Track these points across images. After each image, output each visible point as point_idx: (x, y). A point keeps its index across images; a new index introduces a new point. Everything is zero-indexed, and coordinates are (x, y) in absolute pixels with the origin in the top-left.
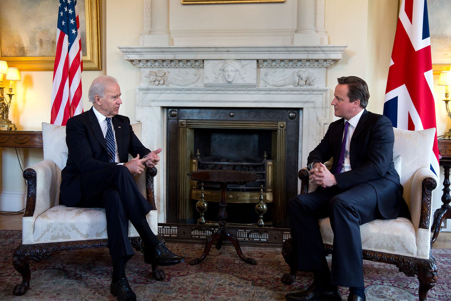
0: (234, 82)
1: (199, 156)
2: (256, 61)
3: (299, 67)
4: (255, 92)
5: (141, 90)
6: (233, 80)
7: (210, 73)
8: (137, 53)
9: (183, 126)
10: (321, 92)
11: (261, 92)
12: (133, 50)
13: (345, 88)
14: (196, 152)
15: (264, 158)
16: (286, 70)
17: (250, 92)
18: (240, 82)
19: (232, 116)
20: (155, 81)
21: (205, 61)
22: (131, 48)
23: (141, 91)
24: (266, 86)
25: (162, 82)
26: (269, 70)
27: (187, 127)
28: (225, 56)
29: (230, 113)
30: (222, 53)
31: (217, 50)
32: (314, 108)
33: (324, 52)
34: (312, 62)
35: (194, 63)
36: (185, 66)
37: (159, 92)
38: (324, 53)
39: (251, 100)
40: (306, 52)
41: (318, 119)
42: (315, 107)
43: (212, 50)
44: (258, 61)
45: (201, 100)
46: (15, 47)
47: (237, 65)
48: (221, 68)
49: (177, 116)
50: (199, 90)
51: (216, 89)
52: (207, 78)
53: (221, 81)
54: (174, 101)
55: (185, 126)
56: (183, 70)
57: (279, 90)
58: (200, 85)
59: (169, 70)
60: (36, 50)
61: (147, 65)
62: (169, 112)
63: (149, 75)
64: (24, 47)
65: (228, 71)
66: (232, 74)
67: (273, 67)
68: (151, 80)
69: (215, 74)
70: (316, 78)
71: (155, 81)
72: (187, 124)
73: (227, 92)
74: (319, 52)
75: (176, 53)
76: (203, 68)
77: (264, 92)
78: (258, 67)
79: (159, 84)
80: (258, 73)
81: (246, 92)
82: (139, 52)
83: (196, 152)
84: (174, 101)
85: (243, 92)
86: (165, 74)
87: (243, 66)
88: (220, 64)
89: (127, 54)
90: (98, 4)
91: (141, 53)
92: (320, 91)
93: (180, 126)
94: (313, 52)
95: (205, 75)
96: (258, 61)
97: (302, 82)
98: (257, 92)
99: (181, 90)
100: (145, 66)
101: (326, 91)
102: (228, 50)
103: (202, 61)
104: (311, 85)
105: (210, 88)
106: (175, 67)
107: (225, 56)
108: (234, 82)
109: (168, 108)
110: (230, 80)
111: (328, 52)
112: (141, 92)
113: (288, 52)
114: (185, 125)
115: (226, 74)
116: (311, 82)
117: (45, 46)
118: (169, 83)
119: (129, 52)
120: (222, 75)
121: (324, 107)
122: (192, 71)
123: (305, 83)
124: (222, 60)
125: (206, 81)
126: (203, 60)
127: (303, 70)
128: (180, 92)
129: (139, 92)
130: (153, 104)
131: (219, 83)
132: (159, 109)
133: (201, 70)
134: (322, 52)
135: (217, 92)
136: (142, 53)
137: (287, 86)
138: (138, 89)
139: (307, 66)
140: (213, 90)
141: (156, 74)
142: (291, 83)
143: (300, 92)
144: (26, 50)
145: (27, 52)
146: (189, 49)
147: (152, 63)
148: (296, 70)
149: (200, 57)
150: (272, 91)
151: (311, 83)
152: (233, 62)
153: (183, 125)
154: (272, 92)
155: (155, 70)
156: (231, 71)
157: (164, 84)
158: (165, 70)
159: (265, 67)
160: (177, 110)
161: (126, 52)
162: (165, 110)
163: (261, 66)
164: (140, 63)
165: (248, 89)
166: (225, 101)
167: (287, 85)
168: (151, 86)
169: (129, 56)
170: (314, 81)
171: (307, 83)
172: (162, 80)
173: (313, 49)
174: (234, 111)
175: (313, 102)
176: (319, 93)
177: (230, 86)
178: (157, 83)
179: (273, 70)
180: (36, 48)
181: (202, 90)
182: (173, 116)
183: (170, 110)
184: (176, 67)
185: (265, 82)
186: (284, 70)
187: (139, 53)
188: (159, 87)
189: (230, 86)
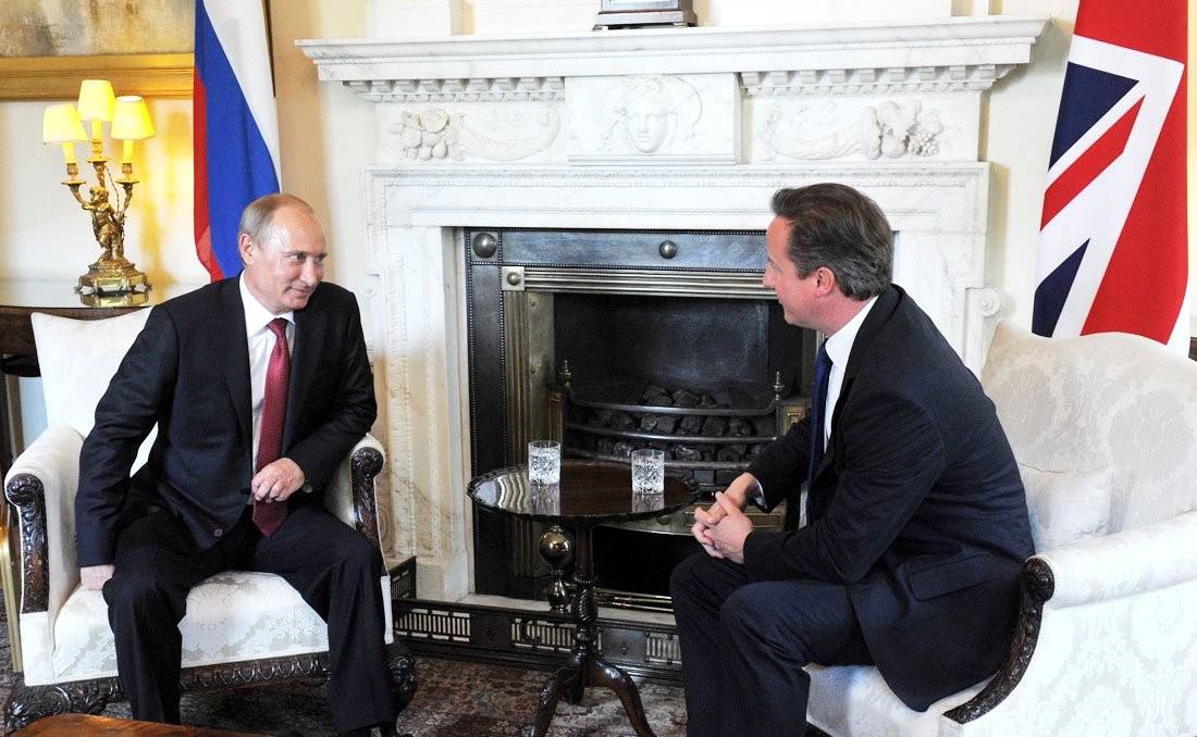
0: (662, 149)
1: (571, 380)
3: (885, 92)
4: (735, 180)
5: (377, 175)
8: (356, 61)
9: (516, 288)
10: (962, 179)
12: (342, 52)
14: (559, 368)
15: (775, 393)
16: (839, 100)
20: (420, 145)
22: (336, 46)
23: (379, 179)
25: (439, 150)
27: (526, 288)
29: (662, 245)
30: (619, 54)
32: (937, 231)
33: (968, 42)
34: (930, 76)
35: (534, 85)
36: (509, 95)
37: (433, 181)
38: (965, 45)
40: (901, 44)
41: (947, 271)
42: (940, 231)
46: (23, 27)
49: (496, 253)
50: (555, 175)
51: (606, 173)
54: (479, 209)
55: (520, 287)
57: (815, 172)
59: (463, 108)
60: (82, 33)
61: (394, 96)
62: (472, 240)
63: (400, 128)
64: (48, 27)
65: (637, 115)
68: (409, 142)
70: (942, 130)
71: (420, 145)
72: (526, 282)
73: (644, 181)
74: (945, 43)
75: (476, 58)
78: (745, 93)
79: (432, 156)
80: (744, 116)
81: (707, 180)
82: (360, 57)
83: (559, 368)
84: (479, 209)
86: (448, 123)
89: (325, 64)
91: (367, 61)
92: (955, 174)
93: (506, 286)
94: (926, 43)
96: (739, 75)
97: (892, 145)
99: (499, 175)
100: (387, 97)
101: (977, 174)
103: (559, 80)
104: (923, 153)
105: (585, 169)
109: (468, 230)
110: (646, 147)
111: (982, 41)
112: (380, 182)
113: (836, 46)
114: (523, 282)
116: (922, 144)
117: (105, 21)
118: (463, 151)
119: (334, 58)
121: (971, 229)
122: (535, 110)
123: (902, 146)
124: (622, 78)
126: (563, 78)
127: (900, 99)
128: (497, 181)
129: (372, 181)
130: (417, 219)
131: (612, 152)
132: (438, 233)
134: (957, 42)
135: (610, 180)
136: (373, 60)
137: (844, 159)
138: (368, 174)
139: (913, 87)
140: (597, 175)
141: (420, 123)
142: (856, 147)
143: (888, 180)
144: (53, 35)
145: (59, 42)
147: (407, 88)
148: (877, 101)
150: (791, 175)
151: (924, 149)
153: (515, 283)
155: (420, 109)
156: (648, 116)
157: (446, 154)
158: (451, 108)
160: (495, 235)
161: (321, 58)
162: (462, 235)
163: (752, 90)
164: (370, 91)
165: (710, 172)
166: (638, 211)
167: (844, 154)
168: (410, 164)
169: (332, 68)
170: (936, 138)
171: (910, 148)
172: (439, 141)
173: (925, 33)
174: (675, 238)
175: (932, 212)
176: (952, 180)
177: (650, 162)
178: (425, 151)
180: (81, 27)
181: (564, 176)
182: (486, 253)
183: (473, 235)
184: (482, 97)
186: (834, 104)
187: (362, 60)
188: (430, 166)
189: (650, 162)
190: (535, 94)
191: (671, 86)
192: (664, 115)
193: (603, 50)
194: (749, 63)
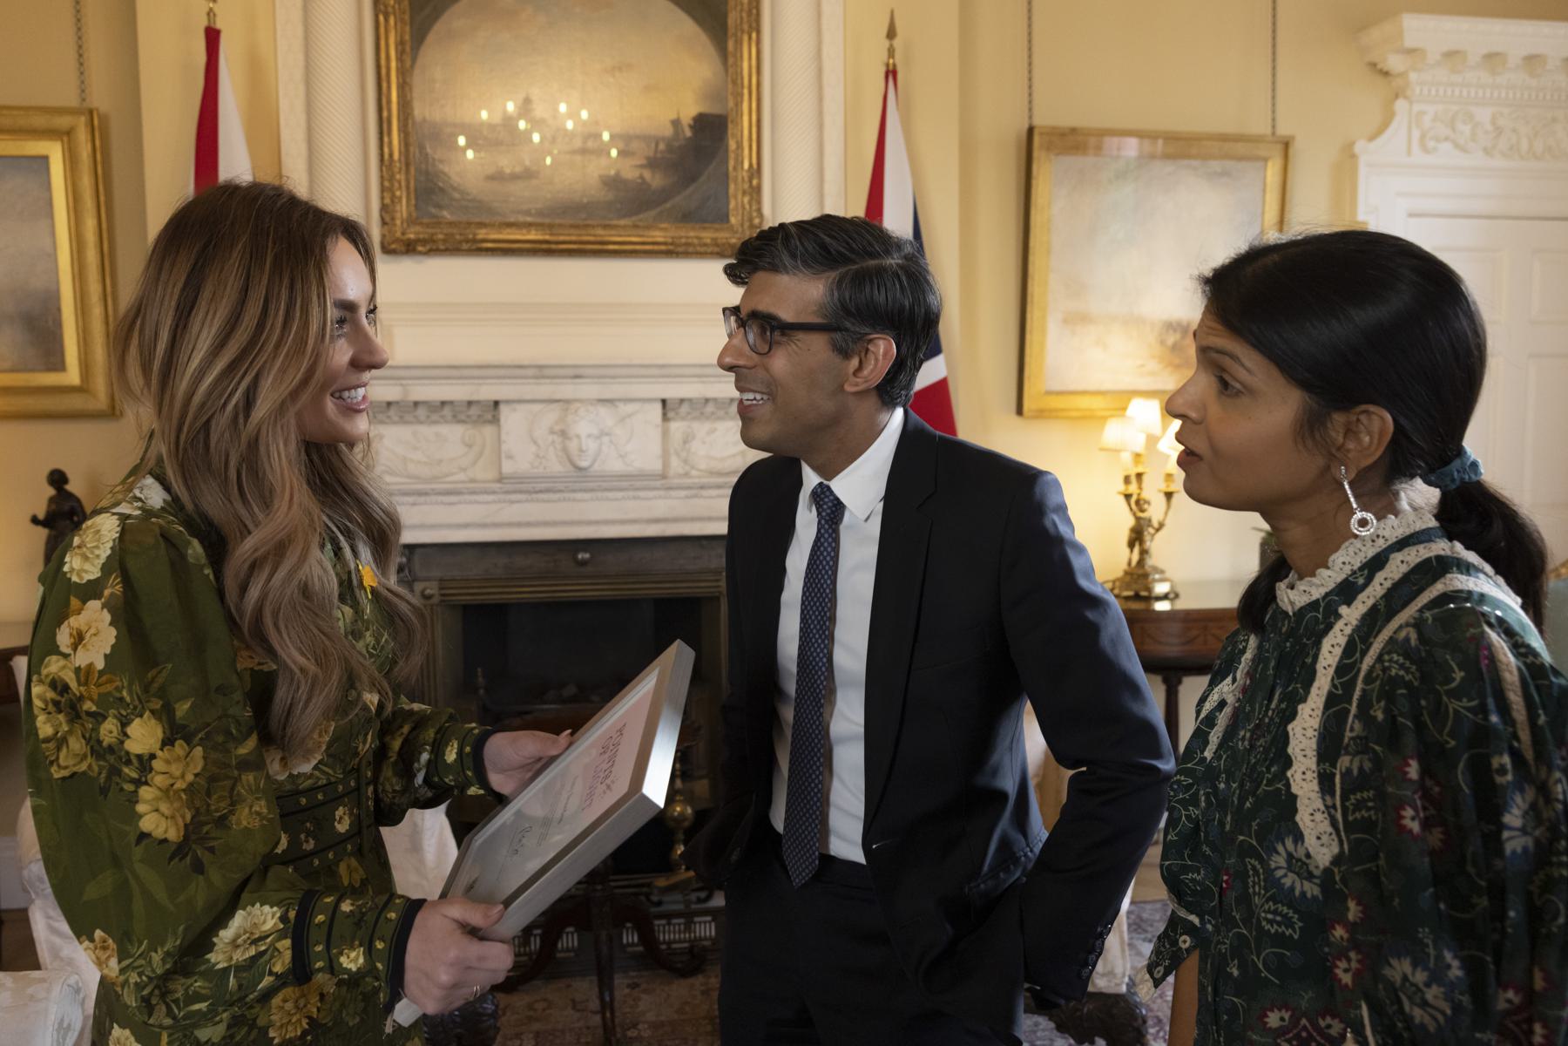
0: (596, 467)
2: (659, 406)
6: (594, 461)
7: (523, 439)
11: (673, 493)
13: (800, 293)
17: (641, 494)
18: (615, 465)
19: (584, 563)
21: (502, 407)
24: (686, 475)
26: (696, 425)
28: (567, 390)
31: (541, 372)
39: (646, 515)
43: (530, 372)
44: (664, 402)
45: (488, 520)
47: (606, 416)
48: (557, 428)
52: (510, 457)
53: (555, 466)
55: (436, 600)
56: (426, 431)
58: (483, 472)
65: (578, 436)
66: (591, 446)
67: (708, 418)
69: (535, 443)
73: (572, 495)
76: (495, 420)
77: (683, 493)
78: (665, 418)
80: (665, 434)
81: (631, 494)
85: (620, 494)
87: (622, 420)
88: (551, 416)
90: (102, 198)
95: (504, 447)
96: (664, 402)
98: (662, 493)
102: (577, 373)
106: (402, 421)
107: (567, 390)
108: (596, 467)
110: (584, 464)
115: (573, 445)
120: (559, 447)
125: (508, 467)
126: (496, 403)
128: (422, 499)
133: (488, 430)
146: (454, 371)
149: (487, 392)
152: (591, 408)
154: (705, 493)
156: (589, 436)
159: (683, 419)
163: (671, 414)
179: (707, 426)
185: (686, 461)
189: (581, 479)
190: (463, 417)
191: (603, 410)
192: (598, 438)
193: (543, 377)
194: (673, 391)
